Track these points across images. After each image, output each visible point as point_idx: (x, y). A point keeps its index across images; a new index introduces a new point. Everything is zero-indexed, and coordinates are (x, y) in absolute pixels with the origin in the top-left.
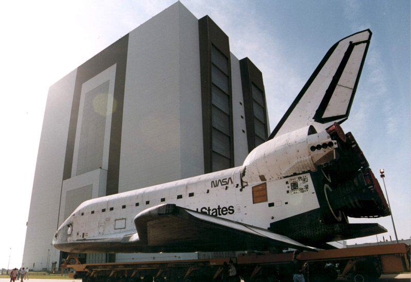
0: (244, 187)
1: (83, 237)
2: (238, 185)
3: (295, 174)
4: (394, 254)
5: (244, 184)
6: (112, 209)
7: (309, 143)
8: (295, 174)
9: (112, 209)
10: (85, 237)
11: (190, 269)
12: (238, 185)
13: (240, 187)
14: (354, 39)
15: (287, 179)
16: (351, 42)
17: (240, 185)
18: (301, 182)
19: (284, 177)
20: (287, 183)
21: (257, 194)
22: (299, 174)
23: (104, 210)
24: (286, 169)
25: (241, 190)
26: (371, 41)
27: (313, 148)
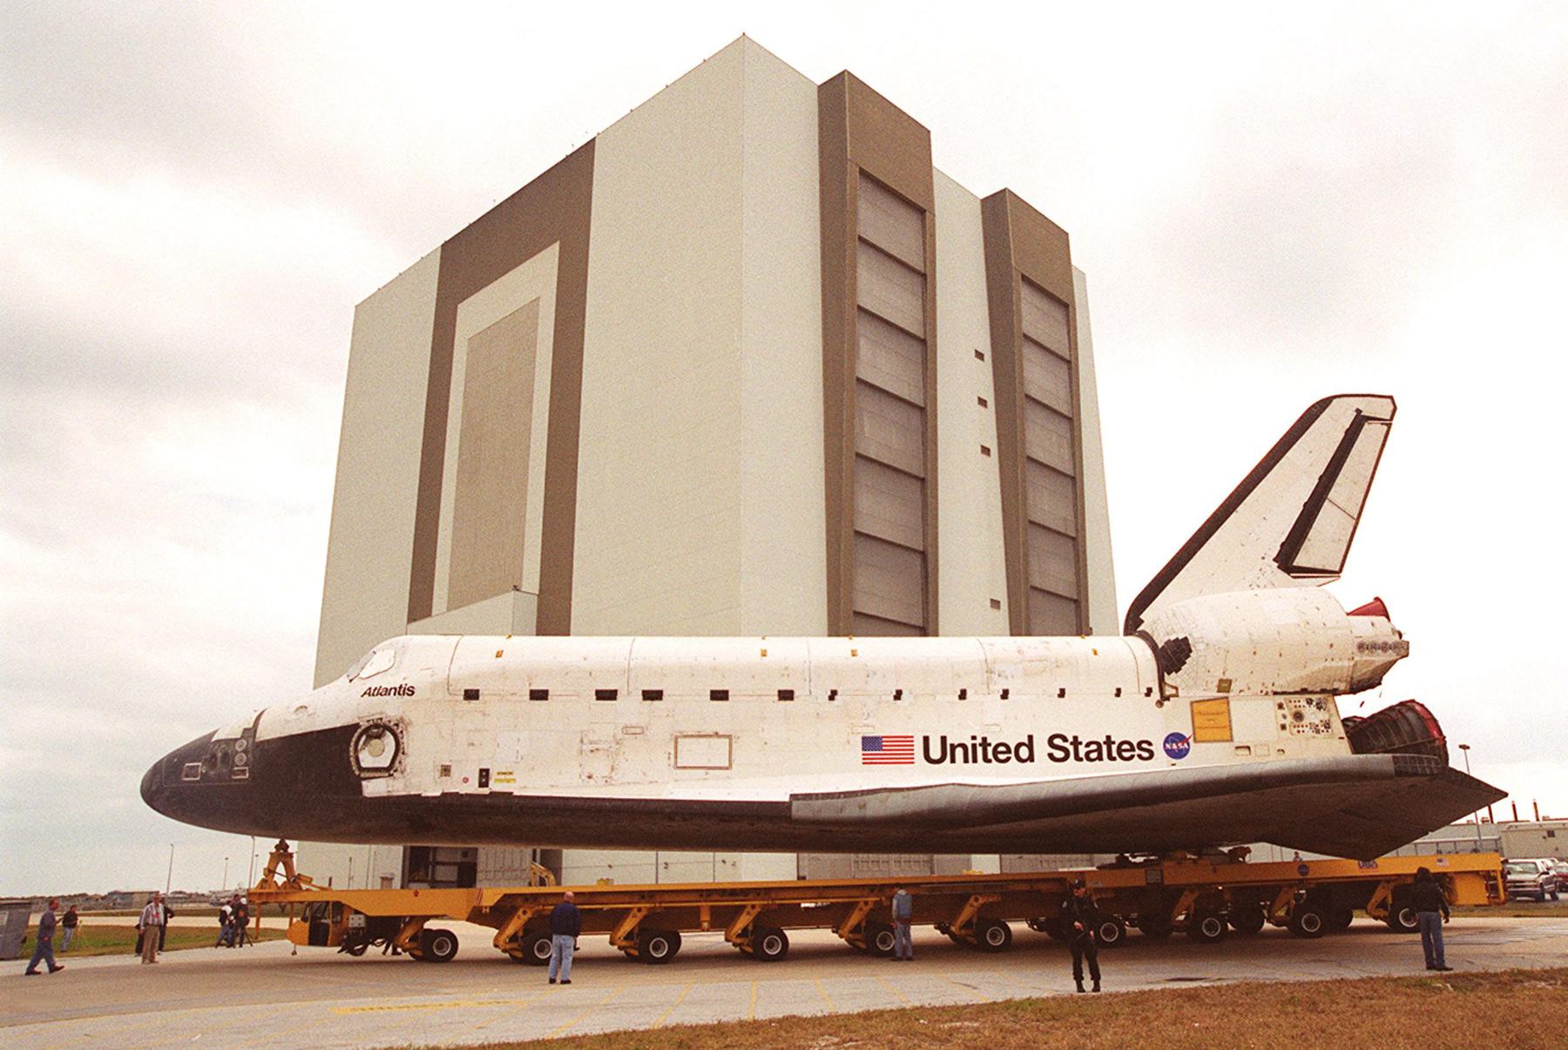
0: (1168, 699)
1: (483, 784)
2: (1149, 691)
3: (1304, 691)
4: (1477, 873)
5: (1169, 691)
6: (652, 695)
7: (1356, 633)
8: (1304, 691)
9: (652, 695)
10: (495, 786)
11: (972, 901)
12: (1149, 691)
13: (1156, 695)
14: (1368, 408)
15: (1280, 699)
16: (1358, 411)
17: (1156, 689)
18: (1313, 708)
19: (1275, 693)
20: (1280, 706)
21: (1223, 720)
22: (1312, 692)
23: (607, 695)
24: (1290, 678)
25: (1160, 704)
26: (1394, 422)
27: (1361, 647)
